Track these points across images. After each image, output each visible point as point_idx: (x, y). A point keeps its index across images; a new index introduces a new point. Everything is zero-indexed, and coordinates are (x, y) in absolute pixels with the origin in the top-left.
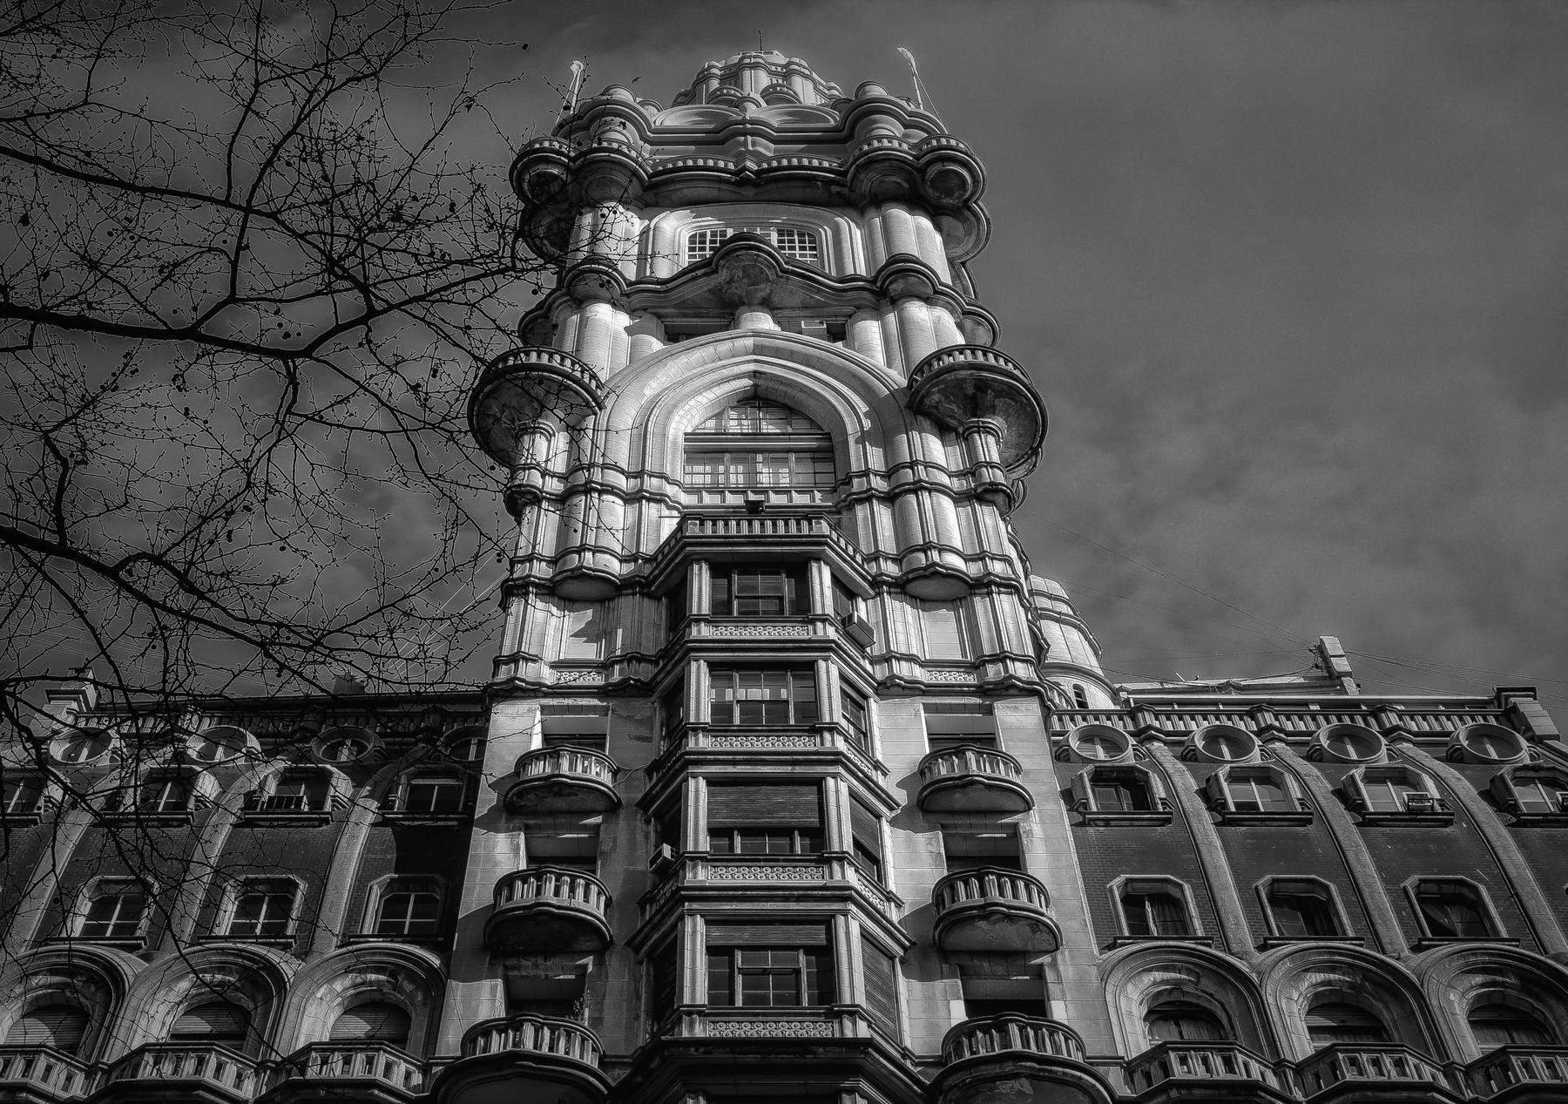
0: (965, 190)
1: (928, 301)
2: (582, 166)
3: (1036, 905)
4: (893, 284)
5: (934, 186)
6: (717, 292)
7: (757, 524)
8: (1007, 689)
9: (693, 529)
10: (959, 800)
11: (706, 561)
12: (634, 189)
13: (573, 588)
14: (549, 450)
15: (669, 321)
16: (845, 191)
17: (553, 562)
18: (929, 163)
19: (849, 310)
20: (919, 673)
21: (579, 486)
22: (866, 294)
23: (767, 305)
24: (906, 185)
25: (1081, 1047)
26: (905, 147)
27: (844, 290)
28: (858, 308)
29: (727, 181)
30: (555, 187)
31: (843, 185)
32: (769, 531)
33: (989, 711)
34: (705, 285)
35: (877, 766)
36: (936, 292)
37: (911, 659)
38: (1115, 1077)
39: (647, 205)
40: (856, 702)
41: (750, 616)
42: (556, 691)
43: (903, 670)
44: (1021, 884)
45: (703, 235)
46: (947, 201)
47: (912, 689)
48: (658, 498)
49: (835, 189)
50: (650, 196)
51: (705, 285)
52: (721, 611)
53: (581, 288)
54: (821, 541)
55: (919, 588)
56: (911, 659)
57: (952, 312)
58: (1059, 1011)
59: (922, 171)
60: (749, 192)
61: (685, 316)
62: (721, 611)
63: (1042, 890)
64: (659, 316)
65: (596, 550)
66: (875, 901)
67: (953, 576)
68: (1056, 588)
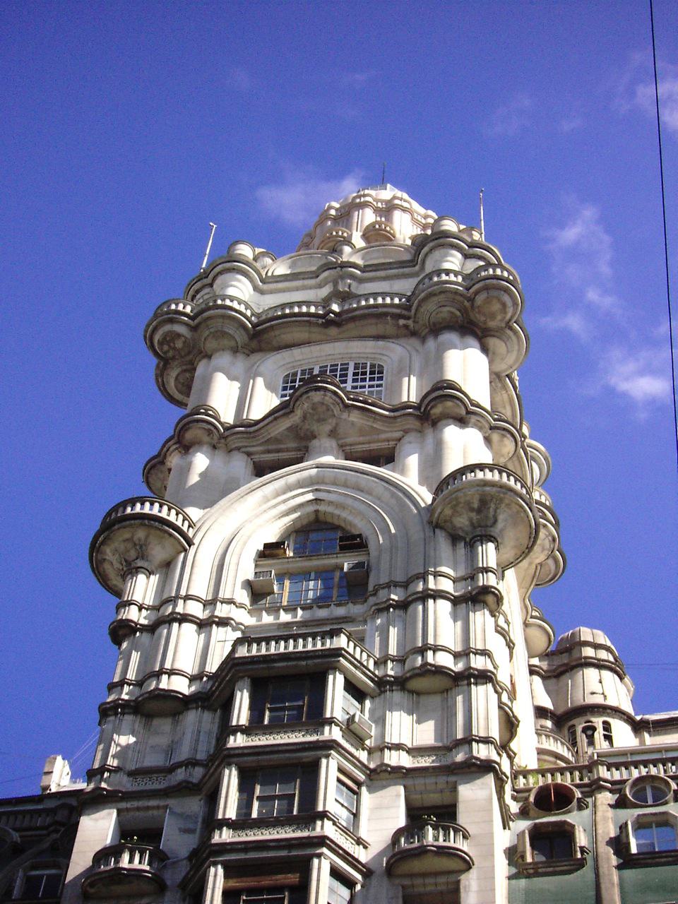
0: (505, 313)
1: (462, 422)
2: (199, 324)
4: (442, 406)
5: (471, 317)
6: (293, 429)
9: (242, 652)
10: (417, 865)
11: (249, 677)
12: (241, 337)
13: (153, 706)
14: (143, 588)
15: (257, 458)
16: (410, 322)
17: (139, 683)
18: (477, 293)
19: (398, 435)
20: (405, 761)
21: (165, 618)
22: (411, 420)
23: (333, 434)
24: (458, 313)
27: (395, 418)
28: (406, 432)
30: (179, 344)
31: (408, 318)
33: (454, 790)
34: (284, 425)
35: (359, 842)
36: (468, 412)
37: (398, 747)
39: (253, 351)
41: (277, 726)
42: (128, 796)
43: (394, 759)
45: (295, 374)
46: (492, 324)
47: (398, 774)
48: (224, 622)
49: (402, 322)
50: (254, 344)
51: (284, 425)
52: (254, 726)
53: (189, 436)
54: (338, 652)
55: (416, 684)
56: (398, 747)
57: (480, 429)
59: (472, 300)
60: (333, 331)
61: (269, 452)
62: (254, 726)
64: (249, 454)
65: (172, 673)
67: (440, 671)
68: (602, 638)
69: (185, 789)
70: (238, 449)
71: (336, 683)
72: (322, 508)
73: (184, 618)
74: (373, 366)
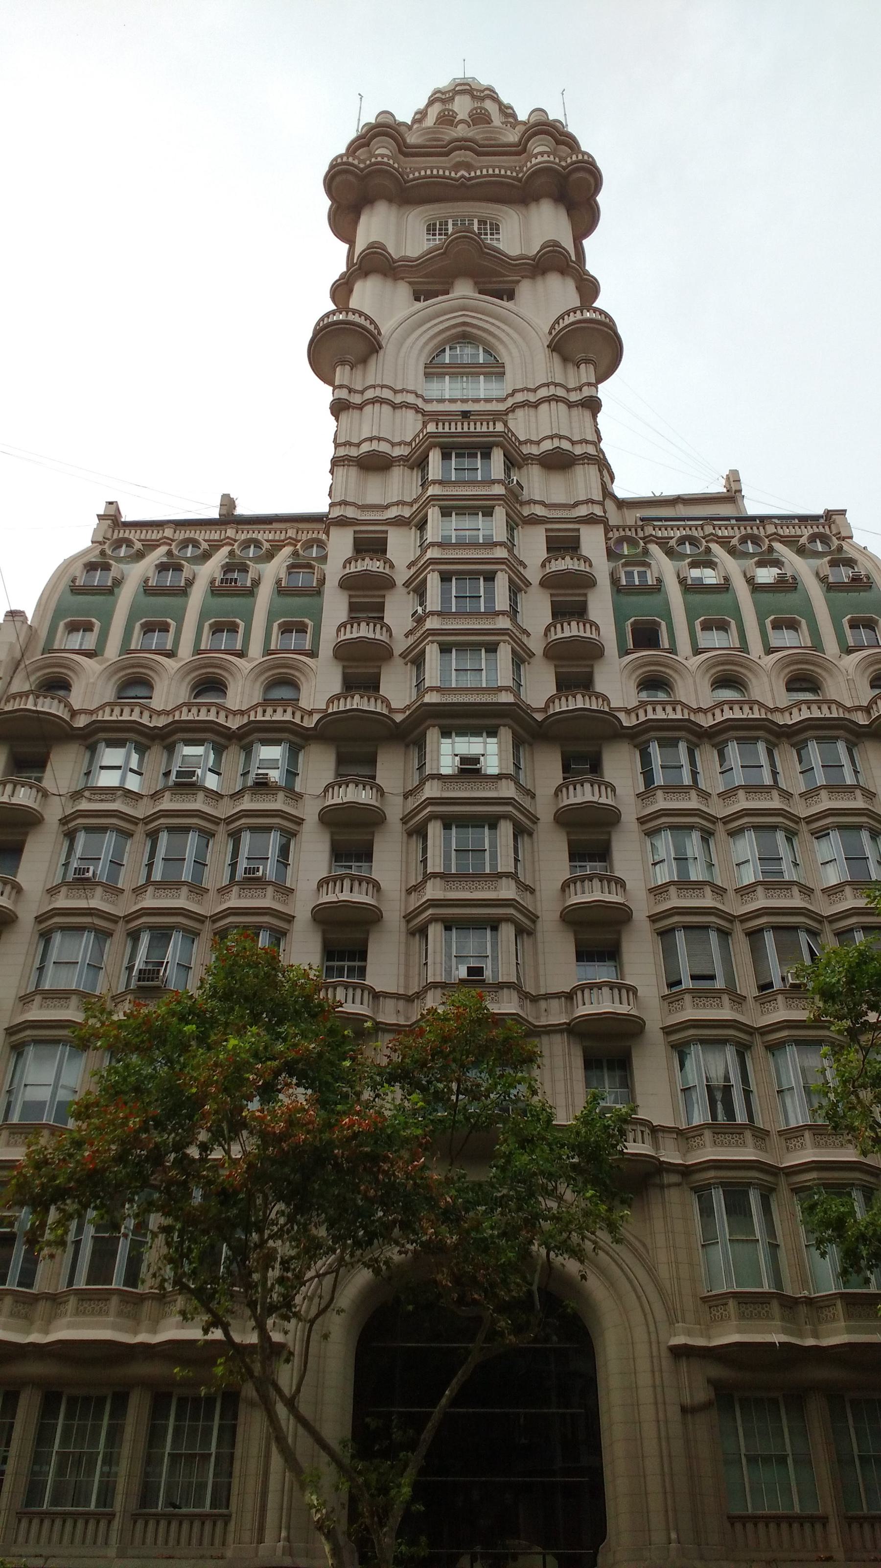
3: (593, 636)
7: (466, 424)
8: (591, 520)
9: (431, 428)
25: (609, 704)
26: (557, 160)
27: (516, 265)
29: (452, 186)
32: (472, 429)
38: (622, 716)
40: (511, 528)
43: (539, 511)
44: (588, 626)
45: (435, 225)
58: (600, 686)
63: (598, 628)
64: (410, 283)
66: (518, 634)
69: (399, 522)
70: (402, 279)
71: (497, 456)
72: (468, 329)
73: (382, 401)
74: (491, 224)
